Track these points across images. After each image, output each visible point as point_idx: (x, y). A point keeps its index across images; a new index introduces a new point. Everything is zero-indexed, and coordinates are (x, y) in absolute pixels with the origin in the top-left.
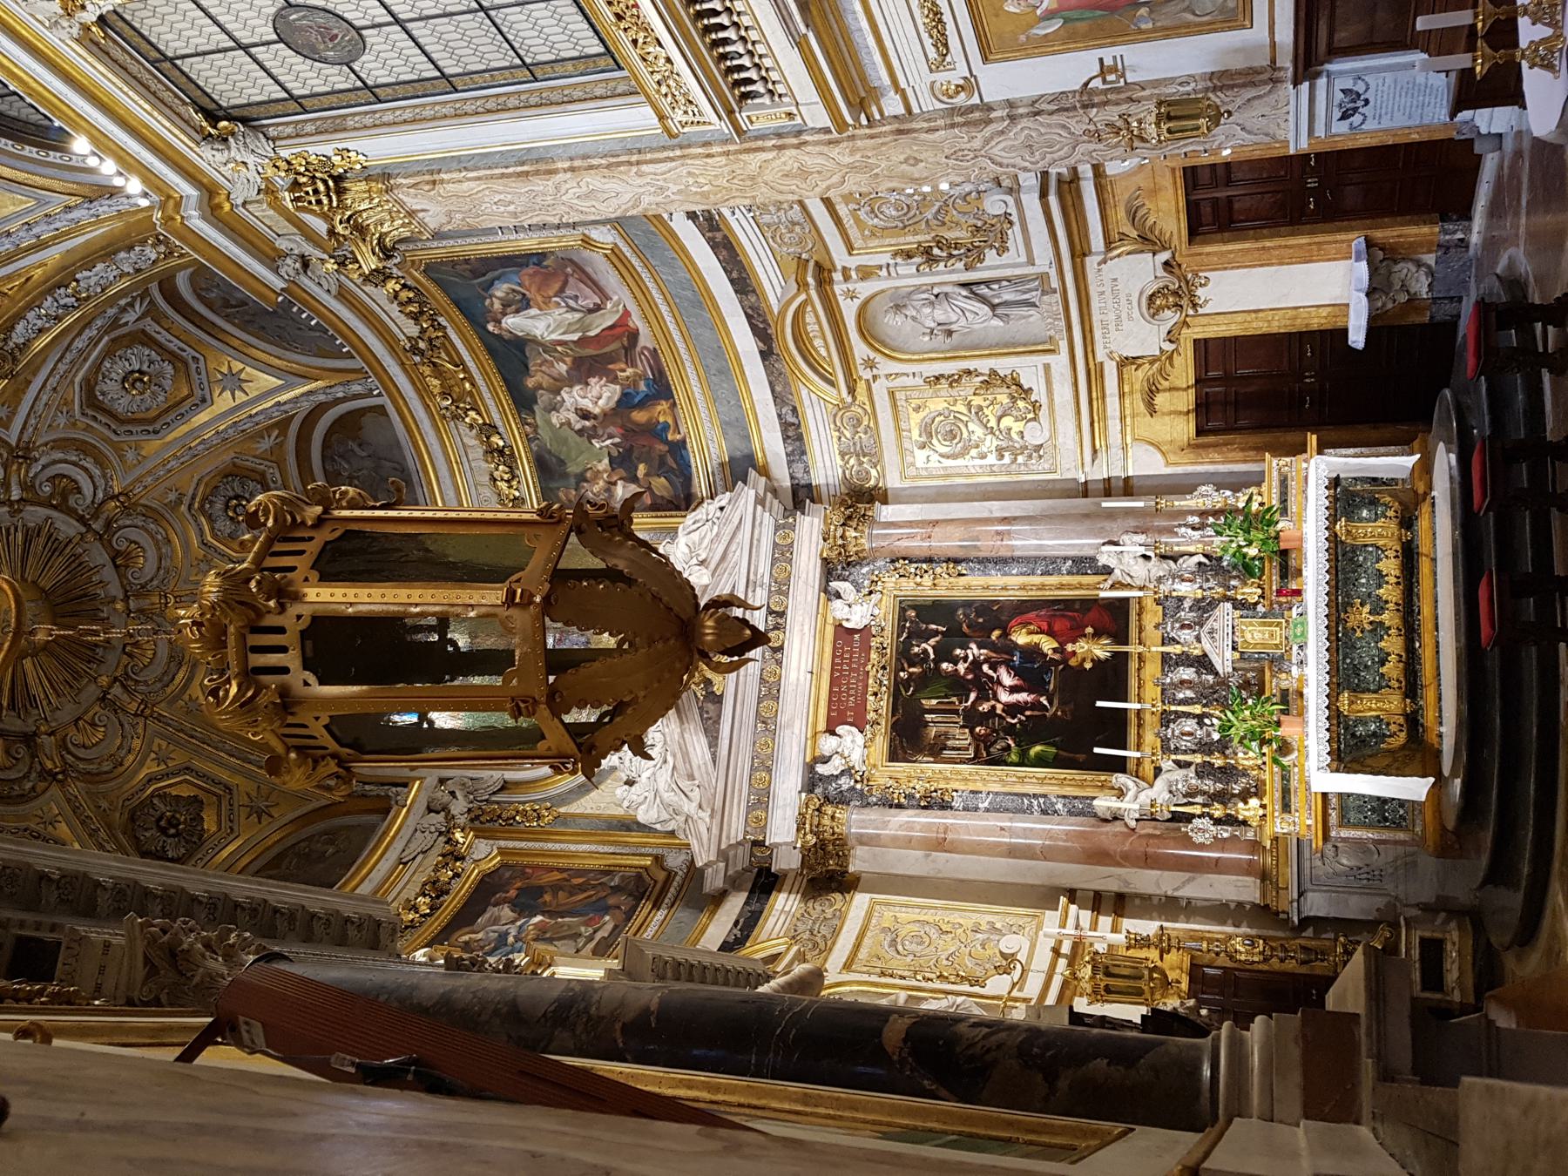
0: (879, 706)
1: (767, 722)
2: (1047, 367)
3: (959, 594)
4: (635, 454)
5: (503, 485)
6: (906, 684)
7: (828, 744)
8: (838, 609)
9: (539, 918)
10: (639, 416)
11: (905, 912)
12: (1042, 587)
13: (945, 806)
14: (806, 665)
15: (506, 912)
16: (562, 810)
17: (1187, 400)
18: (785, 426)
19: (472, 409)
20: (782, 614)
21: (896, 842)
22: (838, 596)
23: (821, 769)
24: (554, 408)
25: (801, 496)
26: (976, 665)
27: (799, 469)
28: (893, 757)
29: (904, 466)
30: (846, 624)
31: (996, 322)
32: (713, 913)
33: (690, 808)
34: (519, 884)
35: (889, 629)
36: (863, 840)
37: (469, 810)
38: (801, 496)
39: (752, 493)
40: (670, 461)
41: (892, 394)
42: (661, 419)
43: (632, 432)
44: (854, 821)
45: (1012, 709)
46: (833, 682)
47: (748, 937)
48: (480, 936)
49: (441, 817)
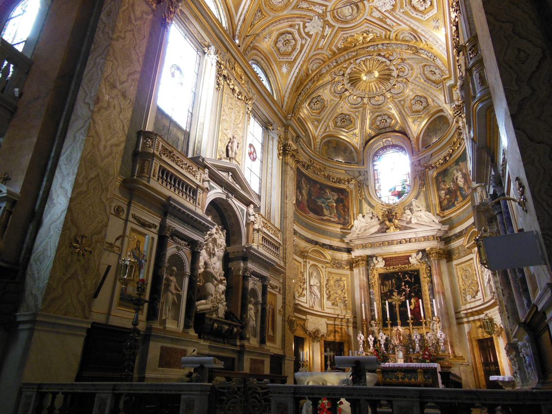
0: (391, 269)
2: (481, 299)
4: (451, 194)
5: (437, 164)
6: (398, 275)
7: (380, 259)
9: (335, 204)
10: (458, 193)
15: (336, 197)
16: (363, 201)
18: (461, 232)
19: (453, 150)
20: (410, 242)
22: (417, 254)
23: (374, 258)
24: (457, 171)
26: (404, 290)
27: (454, 237)
28: (379, 274)
30: (410, 258)
31: (486, 284)
32: (340, 241)
34: (344, 197)
35: (410, 268)
37: (361, 180)
39: (440, 228)
40: (451, 203)
41: (472, 259)
42: (459, 199)
43: (455, 192)
46: (395, 257)
47: (334, 250)
48: (329, 194)
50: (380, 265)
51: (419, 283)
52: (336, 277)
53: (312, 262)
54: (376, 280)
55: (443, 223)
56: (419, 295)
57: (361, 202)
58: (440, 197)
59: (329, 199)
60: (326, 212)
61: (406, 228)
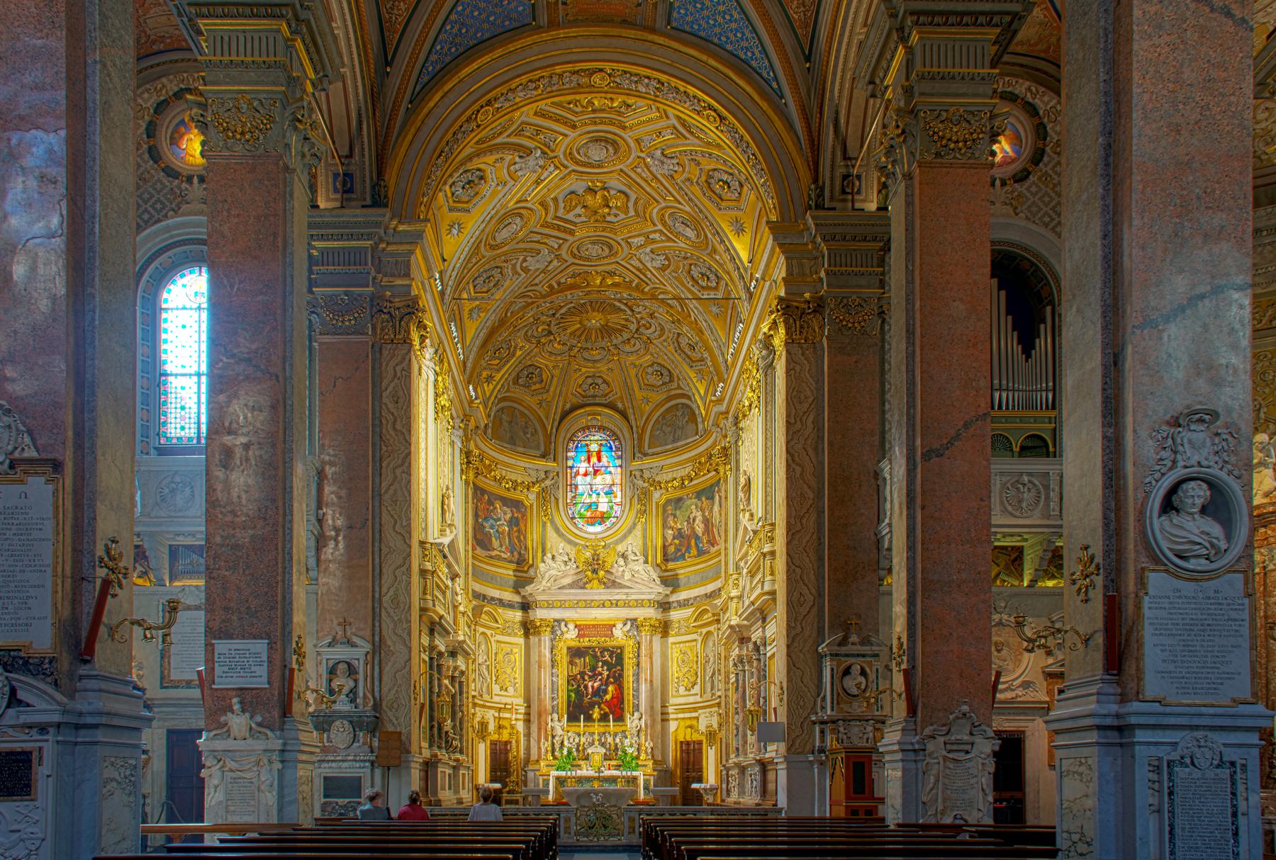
0: (585, 642)
1: (576, 605)
3: (626, 666)
6: (594, 651)
7: (571, 626)
8: (620, 625)
11: (518, 656)
12: (629, 694)
13: (553, 667)
14: (599, 616)
15: (509, 516)
17: (688, 738)
18: (688, 600)
20: (617, 605)
21: (540, 652)
23: (563, 624)
25: (665, 606)
26: (601, 674)
28: (569, 648)
29: (675, 643)
33: (544, 583)
36: (540, 640)
38: (665, 606)
41: (695, 640)
44: (546, 638)
45: (586, 687)
46: (594, 626)
49: (544, 476)
50: (571, 635)
51: (622, 666)
52: (507, 648)
53: (481, 630)
54: (565, 657)
55: (665, 581)
56: (618, 680)
57: (544, 525)
58: (664, 538)
59: (499, 519)
60: (496, 543)
61: (614, 584)
